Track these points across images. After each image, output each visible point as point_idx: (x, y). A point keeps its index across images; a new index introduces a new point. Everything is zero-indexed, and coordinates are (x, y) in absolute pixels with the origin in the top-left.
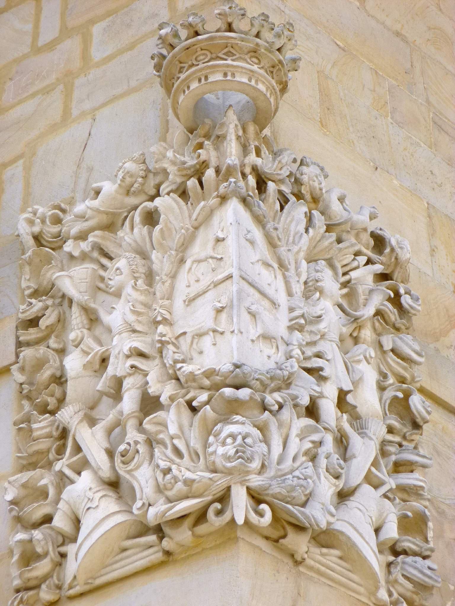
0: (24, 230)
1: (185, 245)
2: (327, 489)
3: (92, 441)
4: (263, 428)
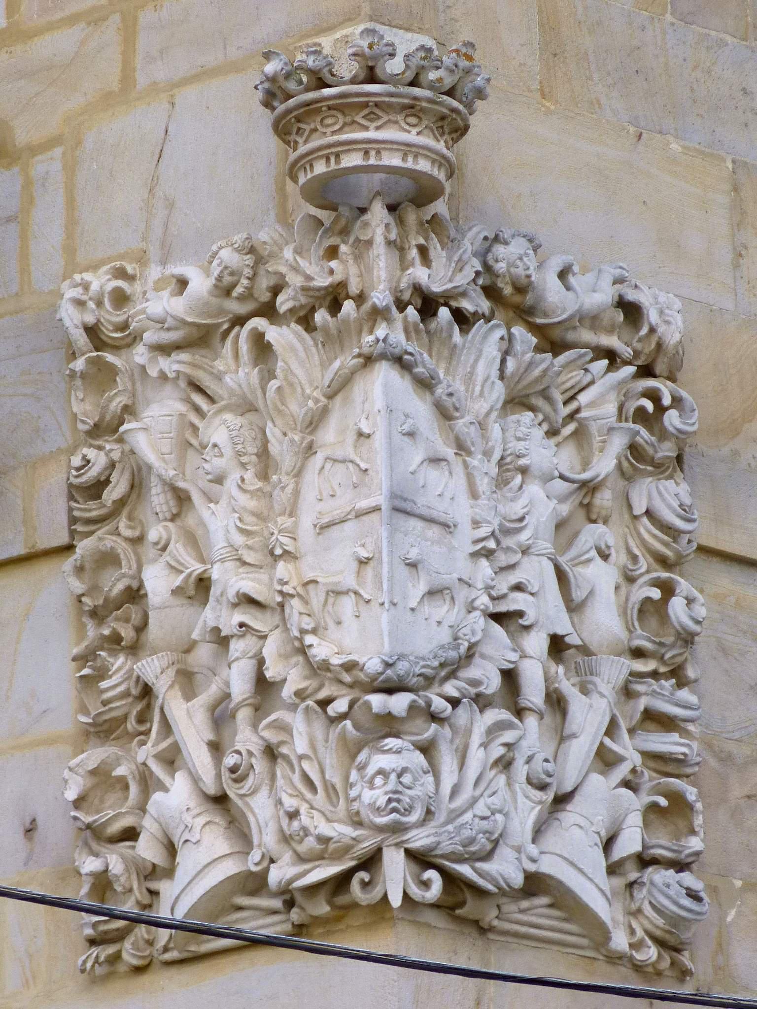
0: (72, 319)
1: (315, 422)
2: (527, 809)
3: (189, 722)
4: (427, 749)
